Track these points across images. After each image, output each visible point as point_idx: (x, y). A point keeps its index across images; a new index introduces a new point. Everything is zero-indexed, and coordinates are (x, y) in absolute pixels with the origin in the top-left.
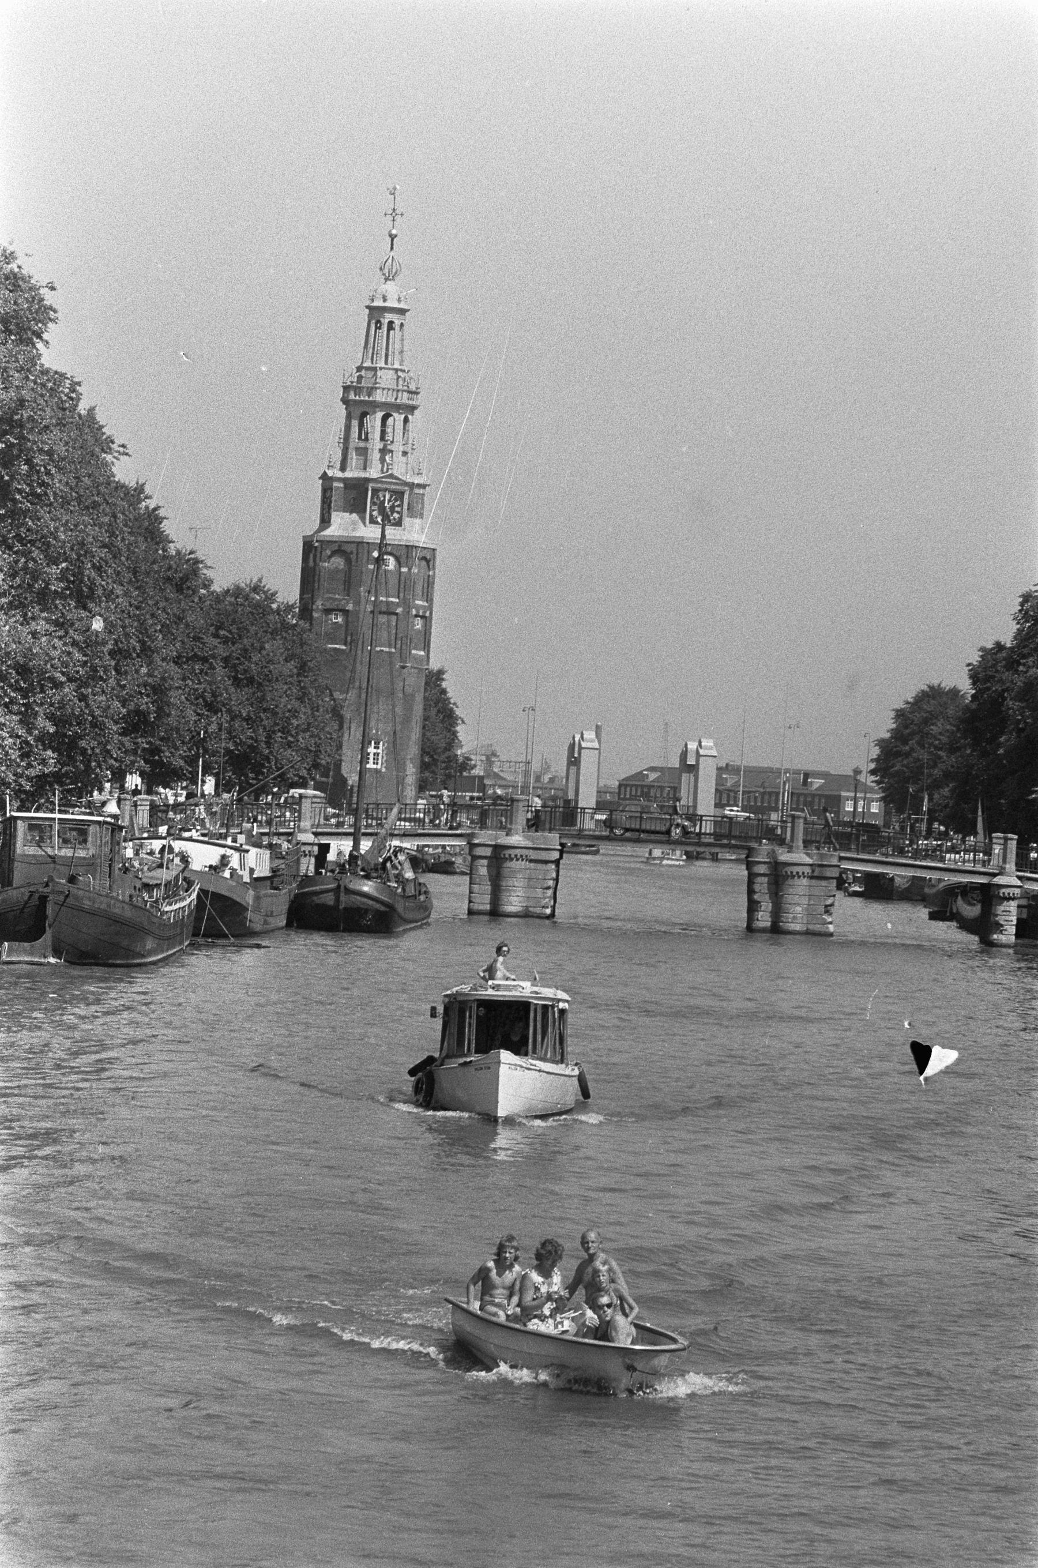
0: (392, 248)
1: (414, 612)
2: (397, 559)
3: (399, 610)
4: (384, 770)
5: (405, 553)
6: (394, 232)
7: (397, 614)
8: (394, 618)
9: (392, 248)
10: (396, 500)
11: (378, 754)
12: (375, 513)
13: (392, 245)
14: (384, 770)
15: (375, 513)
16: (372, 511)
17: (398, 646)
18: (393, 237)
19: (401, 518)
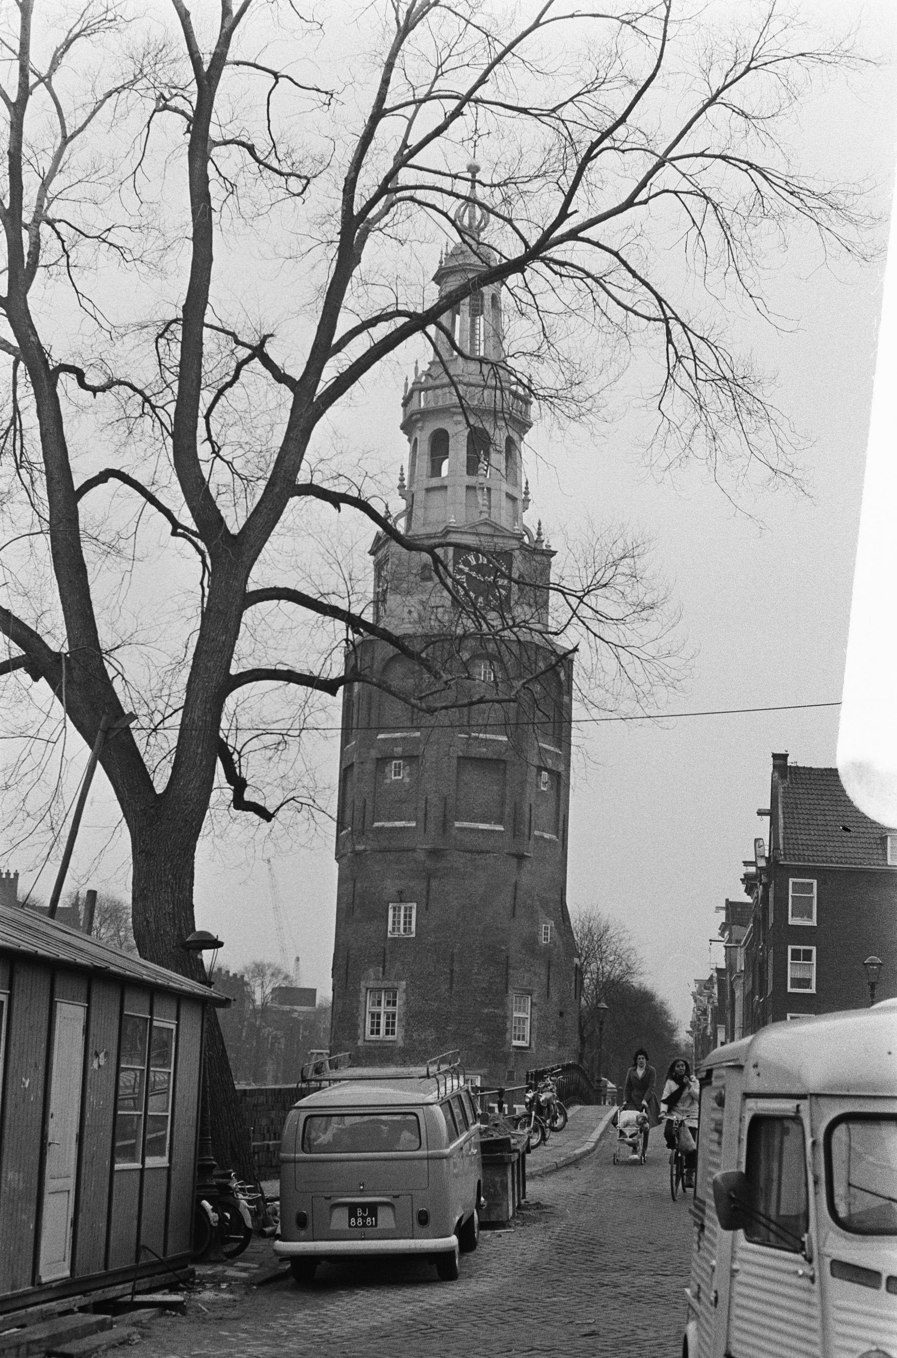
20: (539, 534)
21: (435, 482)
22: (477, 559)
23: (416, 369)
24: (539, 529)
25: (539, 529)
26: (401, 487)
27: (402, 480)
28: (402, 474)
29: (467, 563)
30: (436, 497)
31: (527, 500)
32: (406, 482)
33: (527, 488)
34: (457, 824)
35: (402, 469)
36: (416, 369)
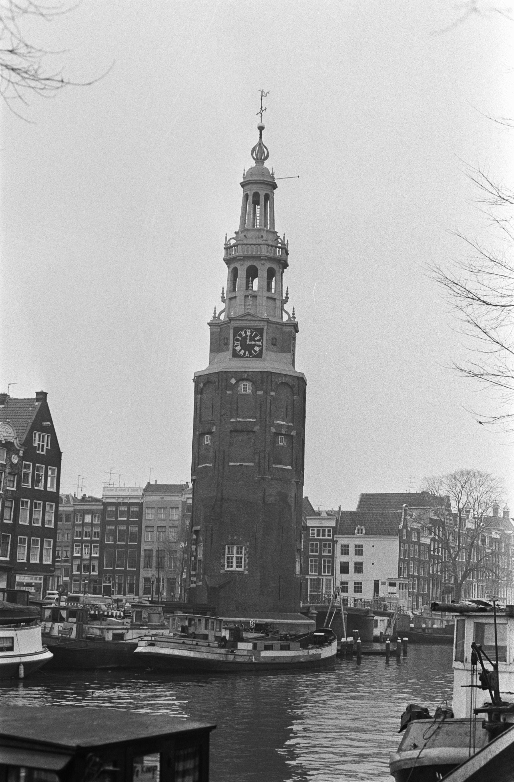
0: (261, 138)
1: (273, 430)
2: (254, 383)
3: (256, 428)
4: (246, 572)
5: (263, 380)
6: (260, 125)
7: (254, 432)
8: (252, 435)
9: (261, 138)
10: (256, 335)
11: (241, 558)
12: (238, 348)
13: (261, 135)
14: (246, 572)
15: (238, 348)
16: (234, 346)
17: (257, 461)
18: (261, 129)
19: (261, 351)
20: (293, 314)
21: (233, 295)
22: (245, 333)
23: (226, 238)
24: (294, 311)
25: (294, 311)
26: (223, 297)
27: (223, 294)
28: (223, 291)
29: (240, 335)
30: (233, 301)
31: (287, 298)
32: (225, 295)
33: (287, 291)
34: (231, 464)
35: (223, 288)
36: (226, 238)
